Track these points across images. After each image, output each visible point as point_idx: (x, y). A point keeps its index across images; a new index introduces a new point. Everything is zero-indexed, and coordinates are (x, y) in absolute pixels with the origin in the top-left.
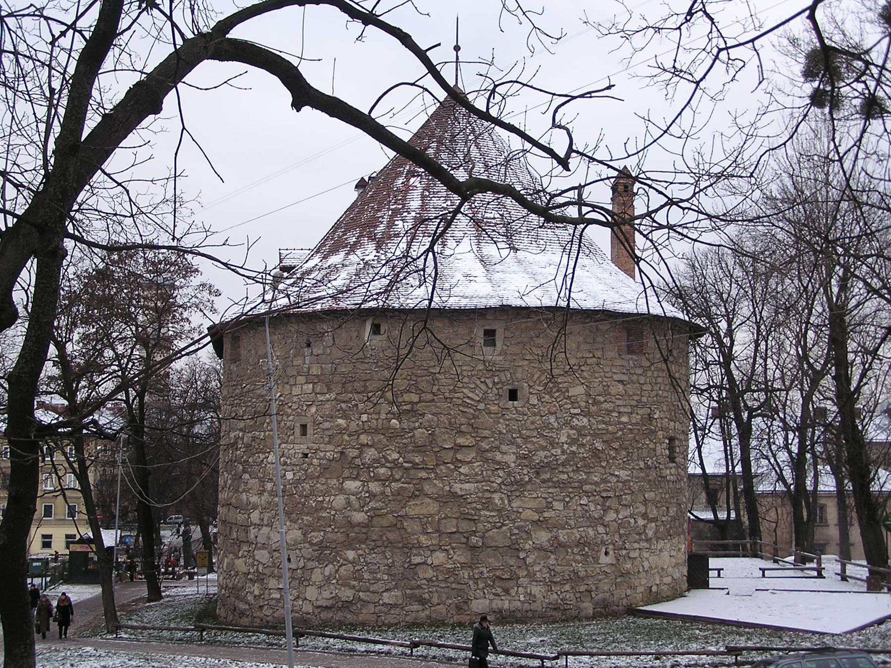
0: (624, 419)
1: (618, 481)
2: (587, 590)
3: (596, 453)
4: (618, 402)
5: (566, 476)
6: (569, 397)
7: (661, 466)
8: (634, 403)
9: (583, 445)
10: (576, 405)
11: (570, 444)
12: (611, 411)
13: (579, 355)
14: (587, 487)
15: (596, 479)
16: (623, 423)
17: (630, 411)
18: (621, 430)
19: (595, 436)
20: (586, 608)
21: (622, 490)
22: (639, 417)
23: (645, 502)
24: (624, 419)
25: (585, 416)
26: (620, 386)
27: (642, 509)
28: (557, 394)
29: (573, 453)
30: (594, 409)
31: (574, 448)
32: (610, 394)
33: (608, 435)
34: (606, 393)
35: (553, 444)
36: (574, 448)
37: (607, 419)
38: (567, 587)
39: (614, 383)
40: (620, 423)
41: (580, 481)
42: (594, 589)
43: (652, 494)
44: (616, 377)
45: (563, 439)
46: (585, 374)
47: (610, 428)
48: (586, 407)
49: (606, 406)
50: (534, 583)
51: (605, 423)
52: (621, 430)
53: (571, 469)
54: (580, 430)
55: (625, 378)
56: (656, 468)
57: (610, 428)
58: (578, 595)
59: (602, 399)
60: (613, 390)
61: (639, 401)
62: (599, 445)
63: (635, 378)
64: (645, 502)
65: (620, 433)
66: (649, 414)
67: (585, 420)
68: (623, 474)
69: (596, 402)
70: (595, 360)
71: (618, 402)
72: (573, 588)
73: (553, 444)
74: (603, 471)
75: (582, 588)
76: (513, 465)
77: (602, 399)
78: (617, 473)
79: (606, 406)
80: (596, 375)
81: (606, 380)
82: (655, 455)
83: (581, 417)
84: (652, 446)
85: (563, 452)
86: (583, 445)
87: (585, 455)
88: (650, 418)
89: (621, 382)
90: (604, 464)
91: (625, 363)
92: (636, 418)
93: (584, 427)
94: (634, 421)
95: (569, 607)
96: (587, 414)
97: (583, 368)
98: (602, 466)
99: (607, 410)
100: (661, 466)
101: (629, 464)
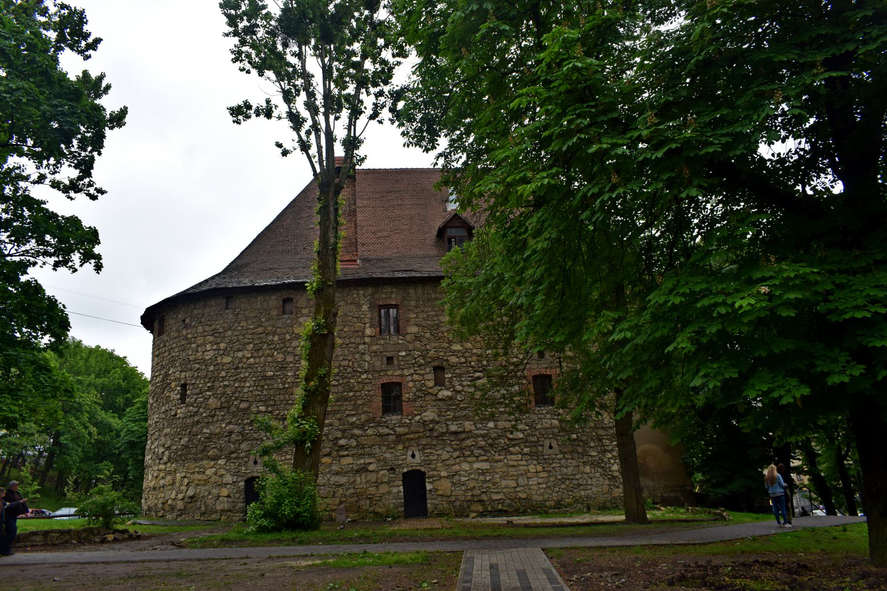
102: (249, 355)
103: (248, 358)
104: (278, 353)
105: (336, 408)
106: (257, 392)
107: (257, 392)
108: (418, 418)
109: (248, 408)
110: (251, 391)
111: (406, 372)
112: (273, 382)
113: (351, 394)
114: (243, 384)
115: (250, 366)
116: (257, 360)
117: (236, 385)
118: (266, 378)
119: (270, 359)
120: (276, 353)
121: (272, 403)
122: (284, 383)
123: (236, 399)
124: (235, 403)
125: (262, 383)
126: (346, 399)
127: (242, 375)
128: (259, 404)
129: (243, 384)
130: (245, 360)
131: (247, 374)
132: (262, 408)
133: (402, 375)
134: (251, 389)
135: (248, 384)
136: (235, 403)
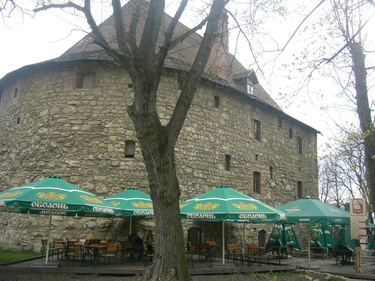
0: (75, 128)
1: (67, 167)
2: (38, 235)
3: (52, 150)
4: (70, 118)
5: (31, 164)
6: (40, 117)
7: (112, 159)
8: (84, 118)
9: (43, 145)
10: (42, 121)
11: (35, 144)
12: (64, 123)
13: (47, 92)
14: (44, 171)
15: (51, 165)
16: (75, 130)
17: (80, 122)
18: (73, 134)
19: (51, 139)
20: (36, 247)
21: (69, 173)
22: (89, 126)
23: (94, 182)
24: (75, 128)
25: (46, 127)
26: (73, 108)
27: (92, 186)
28: (35, 117)
29: (37, 150)
30: (51, 123)
31: (37, 147)
32: (64, 113)
33: (61, 138)
34: (61, 112)
35: (29, 145)
36: (37, 147)
37: (61, 128)
38: (25, 232)
39: (67, 106)
40: (71, 130)
41: (40, 166)
42: (44, 234)
43: (102, 178)
44: (69, 103)
45: (33, 141)
46: (49, 103)
47: (63, 134)
48: (48, 122)
49: (60, 120)
50: (11, 228)
51: (59, 131)
52: (73, 134)
53: (35, 159)
54: (42, 136)
55: (77, 102)
56: (108, 160)
57: (63, 134)
58: (33, 238)
59: (57, 116)
60: (66, 111)
61: (90, 116)
62: (54, 144)
63: (86, 102)
64: (94, 182)
65: (71, 136)
66: (100, 124)
67: (45, 130)
68: (72, 163)
69: (54, 119)
70: (55, 94)
71: (70, 118)
72: (29, 233)
73: (29, 145)
74: (57, 160)
75: (36, 234)
76: (14, 159)
77: (57, 116)
78: (67, 162)
79: (60, 120)
80: (55, 102)
81: (61, 104)
82: (107, 152)
83: (43, 128)
84: (102, 145)
85: (32, 149)
86: (43, 145)
87: (44, 151)
88: (101, 127)
89: (73, 105)
90: (57, 156)
91: (78, 94)
92: (85, 127)
93: (44, 134)
94: (84, 129)
95: (25, 244)
96: (48, 126)
97: (48, 100)
98: (57, 158)
99: (60, 123)
100: (112, 159)
101: (79, 156)
102: (195, 132)
103: (193, 134)
104: (212, 135)
105: (236, 183)
106: (199, 162)
107: (199, 162)
108: (266, 197)
109: (192, 174)
110: (194, 161)
111: (263, 167)
112: (208, 156)
113: (242, 175)
114: (189, 153)
115: (195, 140)
116: (199, 137)
117: (185, 153)
118: (204, 153)
119: (207, 139)
120: (210, 136)
121: (206, 172)
122: (214, 159)
123: (184, 164)
124: (183, 167)
125: (202, 156)
126: (239, 178)
127: (189, 146)
128: (200, 172)
129: (189, 153)
130: (191, 134)
131: (192, 146)
132: (201, 175)
133: (261, 168)
134: (195, 158)
135: (192, 154)
136: (183, 167)
